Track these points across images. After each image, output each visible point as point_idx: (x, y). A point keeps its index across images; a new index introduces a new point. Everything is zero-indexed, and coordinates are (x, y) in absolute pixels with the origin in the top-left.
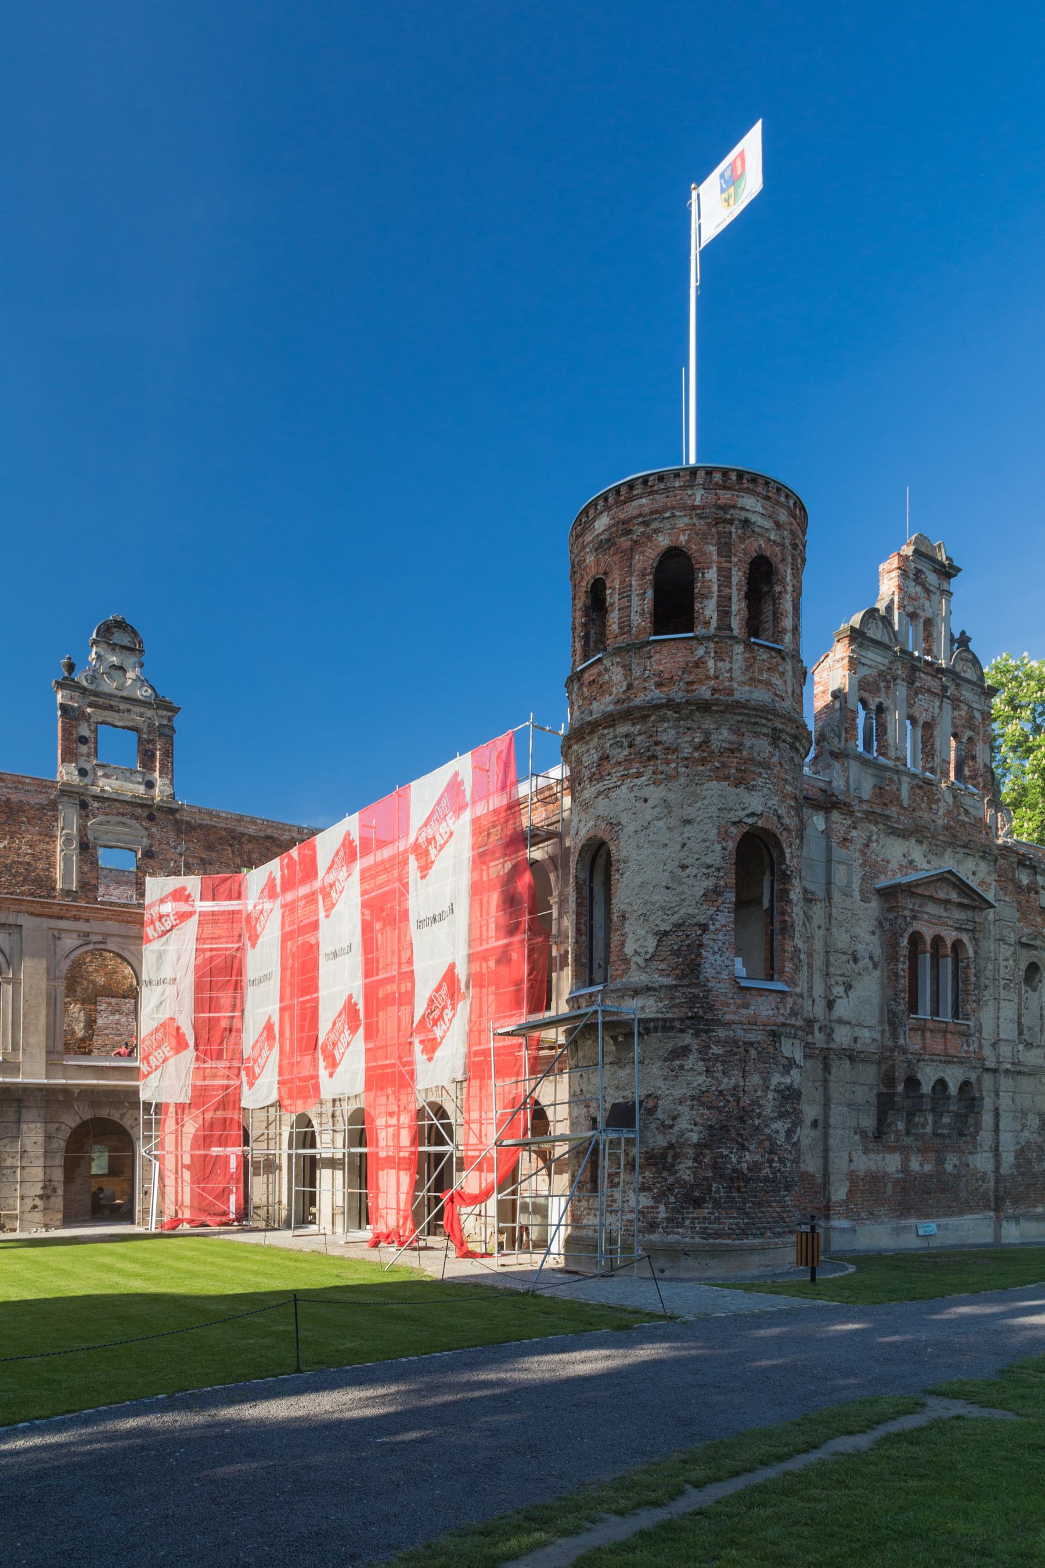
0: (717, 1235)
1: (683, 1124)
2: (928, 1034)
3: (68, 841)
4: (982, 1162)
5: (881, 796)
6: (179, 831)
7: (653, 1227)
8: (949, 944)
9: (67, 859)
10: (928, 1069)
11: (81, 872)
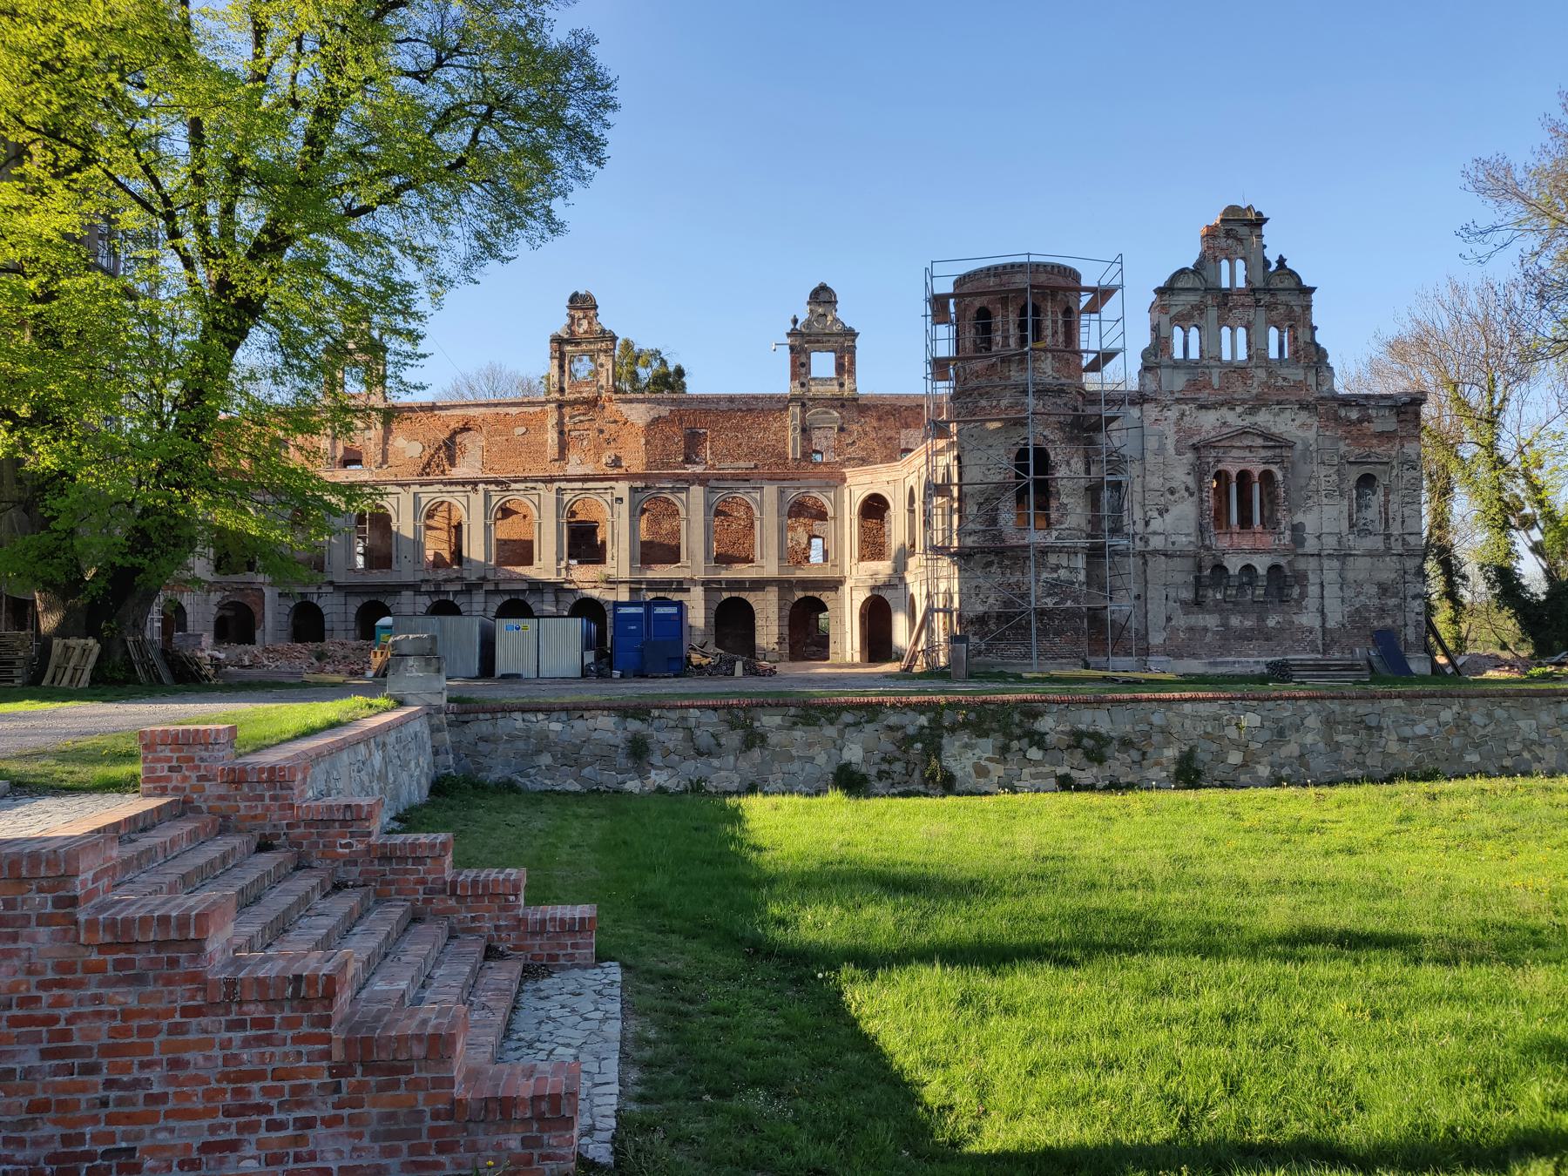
0: (1009, 657)
1: (991, 600)
2: (1235, 536)
3: (795, 429)
4: (1308, 619)
6: (861, 412)
7: (980, 653)
8: (1256, 474)
9: (794, 440)
11: (803, 446)
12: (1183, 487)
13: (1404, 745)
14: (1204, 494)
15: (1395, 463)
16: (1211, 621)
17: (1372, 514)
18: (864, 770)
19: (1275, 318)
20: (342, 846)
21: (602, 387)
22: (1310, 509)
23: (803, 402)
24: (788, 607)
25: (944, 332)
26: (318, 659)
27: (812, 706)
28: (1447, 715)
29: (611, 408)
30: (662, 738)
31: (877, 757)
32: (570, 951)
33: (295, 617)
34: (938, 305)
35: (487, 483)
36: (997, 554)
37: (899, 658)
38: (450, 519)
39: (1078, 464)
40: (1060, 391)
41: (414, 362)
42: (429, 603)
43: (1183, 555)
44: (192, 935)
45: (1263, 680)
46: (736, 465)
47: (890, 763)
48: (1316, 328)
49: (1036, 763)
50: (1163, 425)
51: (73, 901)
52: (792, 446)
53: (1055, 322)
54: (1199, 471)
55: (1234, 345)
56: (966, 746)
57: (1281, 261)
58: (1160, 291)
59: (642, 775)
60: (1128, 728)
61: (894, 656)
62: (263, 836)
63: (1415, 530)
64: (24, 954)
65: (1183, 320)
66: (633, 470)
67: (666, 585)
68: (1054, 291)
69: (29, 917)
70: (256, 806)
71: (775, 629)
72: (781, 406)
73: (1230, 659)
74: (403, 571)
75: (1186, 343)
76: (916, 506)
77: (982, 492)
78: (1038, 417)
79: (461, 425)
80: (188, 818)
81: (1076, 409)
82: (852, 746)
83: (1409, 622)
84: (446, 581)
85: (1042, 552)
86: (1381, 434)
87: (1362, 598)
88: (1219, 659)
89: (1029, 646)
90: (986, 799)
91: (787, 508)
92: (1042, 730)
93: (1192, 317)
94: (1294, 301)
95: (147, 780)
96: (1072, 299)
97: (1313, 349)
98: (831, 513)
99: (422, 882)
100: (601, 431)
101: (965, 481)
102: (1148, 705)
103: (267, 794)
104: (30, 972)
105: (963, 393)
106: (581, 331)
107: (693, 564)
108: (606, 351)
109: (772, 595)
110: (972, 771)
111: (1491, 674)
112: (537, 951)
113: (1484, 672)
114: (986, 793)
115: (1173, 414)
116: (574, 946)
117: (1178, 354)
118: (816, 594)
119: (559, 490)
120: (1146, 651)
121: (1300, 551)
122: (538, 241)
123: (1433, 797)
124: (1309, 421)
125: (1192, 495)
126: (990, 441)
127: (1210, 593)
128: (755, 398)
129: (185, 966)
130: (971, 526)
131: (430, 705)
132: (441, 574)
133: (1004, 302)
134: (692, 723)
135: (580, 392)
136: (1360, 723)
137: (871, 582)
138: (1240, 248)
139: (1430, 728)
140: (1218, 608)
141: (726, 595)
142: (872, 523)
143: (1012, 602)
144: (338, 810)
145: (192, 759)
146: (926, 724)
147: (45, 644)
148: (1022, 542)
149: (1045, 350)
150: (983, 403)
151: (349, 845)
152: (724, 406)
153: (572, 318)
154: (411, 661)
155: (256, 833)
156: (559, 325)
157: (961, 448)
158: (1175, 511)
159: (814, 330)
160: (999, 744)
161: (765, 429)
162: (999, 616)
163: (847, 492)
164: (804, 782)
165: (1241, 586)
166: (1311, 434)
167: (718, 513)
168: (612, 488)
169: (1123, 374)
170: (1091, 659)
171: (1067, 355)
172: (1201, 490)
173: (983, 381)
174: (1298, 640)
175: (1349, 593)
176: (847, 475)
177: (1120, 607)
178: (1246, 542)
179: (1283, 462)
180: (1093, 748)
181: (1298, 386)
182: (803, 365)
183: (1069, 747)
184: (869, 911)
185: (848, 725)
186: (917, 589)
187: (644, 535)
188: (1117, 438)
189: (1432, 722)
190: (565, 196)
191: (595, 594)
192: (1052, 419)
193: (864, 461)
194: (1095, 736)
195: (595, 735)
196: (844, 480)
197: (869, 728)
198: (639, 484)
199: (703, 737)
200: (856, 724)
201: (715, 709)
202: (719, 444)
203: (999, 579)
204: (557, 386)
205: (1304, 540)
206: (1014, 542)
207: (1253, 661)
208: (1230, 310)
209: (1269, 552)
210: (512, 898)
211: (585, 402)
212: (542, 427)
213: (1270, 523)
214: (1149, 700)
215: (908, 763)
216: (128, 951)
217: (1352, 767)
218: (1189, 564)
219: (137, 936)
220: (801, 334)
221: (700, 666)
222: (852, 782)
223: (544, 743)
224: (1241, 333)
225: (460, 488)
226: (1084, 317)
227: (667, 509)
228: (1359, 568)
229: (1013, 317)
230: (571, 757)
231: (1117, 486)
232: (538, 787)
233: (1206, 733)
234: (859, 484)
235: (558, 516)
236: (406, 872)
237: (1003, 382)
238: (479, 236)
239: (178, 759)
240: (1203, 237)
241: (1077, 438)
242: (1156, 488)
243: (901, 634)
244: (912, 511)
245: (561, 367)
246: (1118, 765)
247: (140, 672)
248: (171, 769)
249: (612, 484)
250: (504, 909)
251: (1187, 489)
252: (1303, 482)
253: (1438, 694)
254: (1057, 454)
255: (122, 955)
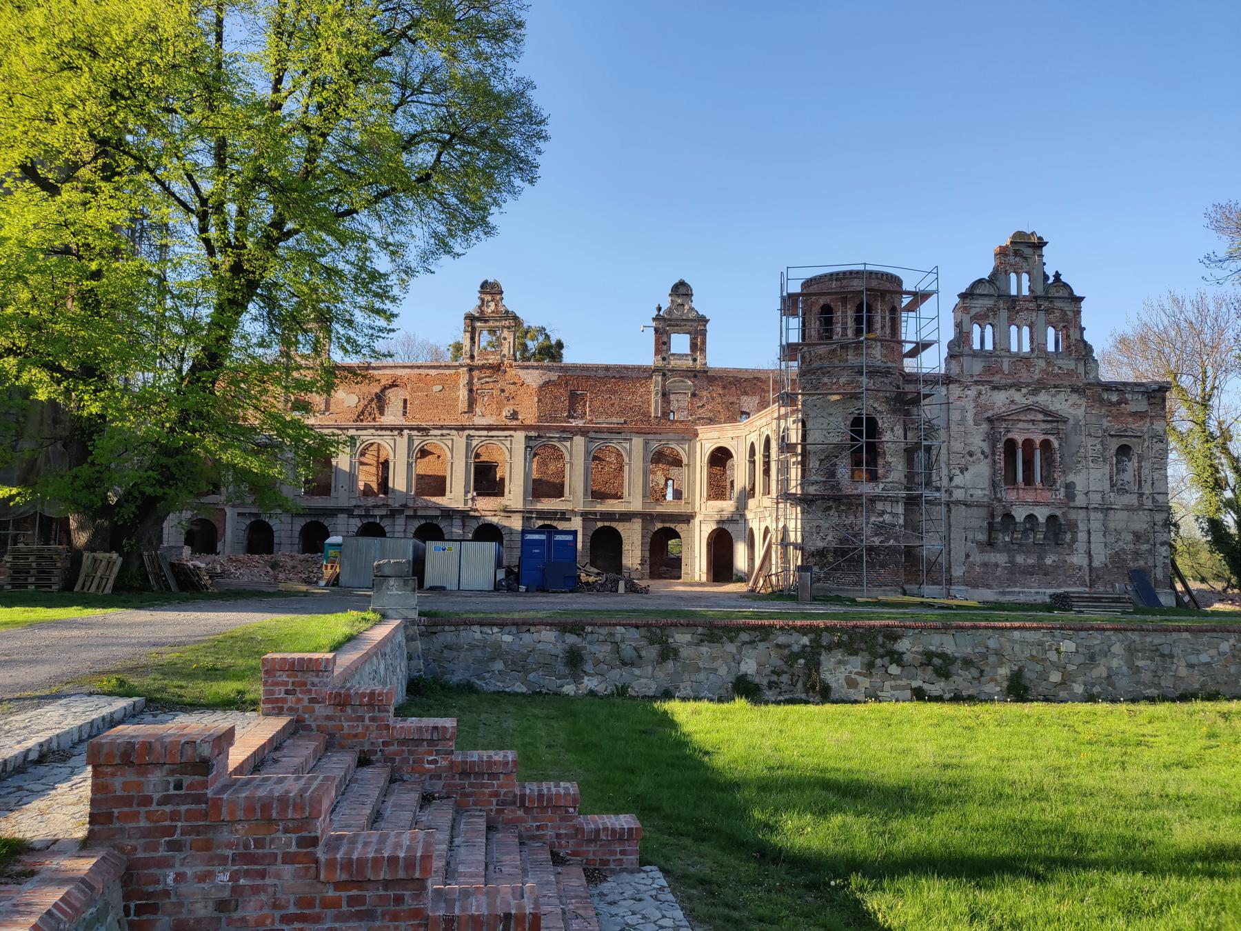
0: (843, 584)
2: (1021, 491)
3: (657, 394)
4: (1078, 559)
5: (989, 370)
7: (819, 580)
8: (1038, 442)
9: (656, 402)
10: (1020, 510)
11: (662, 407)
12: (980, 450)
13: (1190, 670)
14: (997, 457)
15: (1146, 437)
16: (1001, 558)
17: (1128, 476)
18: (757, 680)
19: (1053, 320)
20: (429, 762)
21: (504, 356)
22: (1080, 471)
23: (663, 372)
24: (650, 535)
25: (795, 323)
26: (273, 567)
27: (716, 627)
28: (1225, 647)
29: (511, 372)
30: (593, 650)
31: (768, 670)
32: (619, 857)
33: (250, 532)
34: (790, 304)
35: (411, 429)
36: (835, 501)
37: (741, 580)
38: (378, 457)
39: (899, 431)
40: (887, 373)
41: (385, 335)
42: (359, 524)
43: (979, 505)
44: (417, 875)
45: (1048, 608)
46: (609, 420)
47: (779, 674)
48: (1084, 329)
49: (896, 677)
50: (964, 402)
51: (314, 841)
52: (654, 406)
53: (883, 318)
54: (992, 438)
55: (1019, 340)
56: (840, 662)
57: (1057, 276)
58: (963, 296)
59: (577, 680)
60: (969, 650)
61: (734, 577)
62: (362, 752)
63: (1162, 491)
64: (271, 890)
65: (980, 319)
66: (527, 422)
67: (552, 515)
68: (883, 294)
69: (275, 855)
70: (358, 726)
71: (638, 553)
72: (646, 375)
73: (1016, 589)
74: (340, 498)
75: (982, 337)
76: (757, 458)
77: (823, 451)
78: (870, 392)
79: (390, 382)
80: (301, 736)
81: (898, 387)
82: (747, 660)
83: (1158, 564)
84: (374, 507)
85: (871, 500)
86: (1135, 413)
87: (1121, 543)
88: (1008, 590)
89: (860, 576)
90: (857, 707)
91: (650, 456)
92: (901, 650)
93: (988, 317)
94: (1068, 307)
95: (267, 701)
96: (896, 300)
97: (1082, 345)
98: (685, 461)
99: (496, 794)
100: (503, 391)
101: (809, 441)
102: (985, 632)
103: (367, 716)
104: (275, 906)
105: (809, 371)
106: (489, 311)
107: (574, 499)
108: (509, 328)
109: (637, 525)
110: (844, 683)
111: (1218, 606)
112: (591, 857)
113: (1212, 605)
114: (856, 702)
115: (972, 393)
116: (623, 852)
117: (976, 346)
118: (672, 526)
119: (469, 437)
120: (950, 582)
121: (1071, 505)
122: (474, 241)
123: (1225, 716)
124: (1079, 402)
125: (986, 457)
126: (830, 410)
127: (1000, 536)
128: (626, 368)
129: (409, 903)
130: (814, 478)
131: (405, 618)
132: (371, 501)
133: (844, 301)
134: (618, 638)
135: (487, 359)
136: (1156, 651)
137: (718, 517)
138: (1025, 264)
139: (1212, 657)
140: (1007, 549)
141: (600, 524)
142: (717, 470)
143: (847, 540)
144: (427, 731)
145: (305, 684)
146: (808, 643)
147: (76, 557)
148: (855, 492)
149: (876, 340)
150: (825, 380)
151: (435, 762)
152: (601, 373)
153: (482, 300)
154: (392, 582)
155: (357, 749)
156: (472, 306)
157: (805, 414)
158: (973, 470)
159: (674, 316)
160: (866, 661)
161: (633, 393)
162: (836, 550)
163: (698, 445)
164: (709, 690)
165: (1025, 532)
166: (1080, 412)
167: (595, 458)
168: (511, 436)
169: (932, 362)
170: (906, 587)
171: (893, 344)
172: (994, 454)
173: (826, 363)
174: (1070, 576)
175: (1111, 539)
176: (699, 431)
177: (930, 545)
178: (1029, 497)
179: (1058, 433)
180: (941, 666)
181: (1070, 374)
182: (664, 343)
183: (922, 664)
184: (837, 820)
185: (744, 643)
186: (757, 527)
187: (535, 475)
188: (929, 411)
189: (1213, 652)
190: (500, 207)
191: (495, 520)
192: (880, 394)
193: (711, 421)
194: (943, 656)
195: (539, 646)
196: (696, 435)
197: (762, 646)
198: (533, 434)
199: (627, 651)
200: (752, 642)
201: (637, 627)
202: (597, 404)
203: (836, 520)
204: (469, 354)
205: (1075, 495)
206: (849, 492)
207: (1039, 592)
208: (1017, 313)
209: (1047, 504)
210: (571, 810)
211: (491, 367)
212: (455, 386)
213: (1049, 481)
214: (986, 628)
215: (793, 675)
216: (360, 889)
217: (1150, 687)
218: (983, 512)
219: (370, 875)
220: (663, 319)
221: (587, 584)
222: (746, 689)
223: (497, 652)
224: (1026, 330)
225: (388, 433)
226: (904, 314)
227: (553, 454)
228: (1118, 519)
229: (851, 313)
230: (519, 664)
231: (928, 449)
232: (492, 689)
233: (1031, 655)
234: (709, 439)
235: (467, 458)
236: (482, 785)
237: (842, 364)
238: (435, 235)
239: (293, 683)
240: (996, 255)
241: (899, 410)
242: (959, 450)
243: (741, 560)
244: (753, 462)
245: (472, 339)
246: (962, 680)
247: (153, 582)
248: (287, 692)
249: (512, 433)
250: (563, 819)
251: (983, 452)
252: (1074, 450)
253: (1218, 629)
254: (883, 423)
255: (355, 892)
